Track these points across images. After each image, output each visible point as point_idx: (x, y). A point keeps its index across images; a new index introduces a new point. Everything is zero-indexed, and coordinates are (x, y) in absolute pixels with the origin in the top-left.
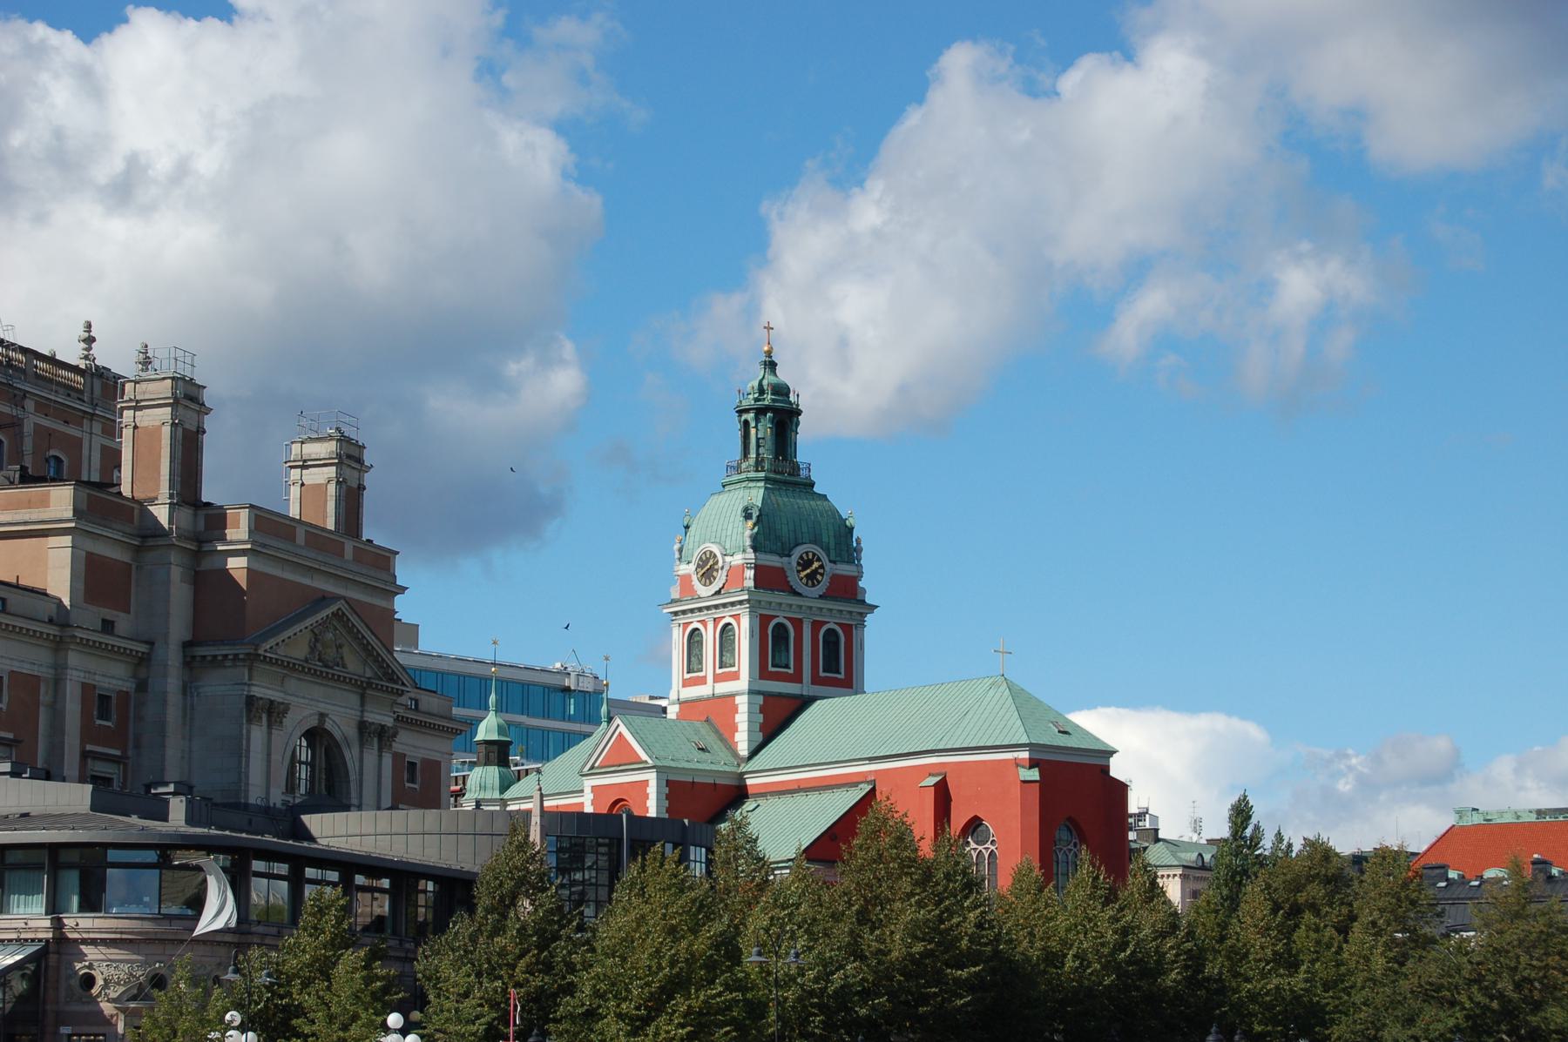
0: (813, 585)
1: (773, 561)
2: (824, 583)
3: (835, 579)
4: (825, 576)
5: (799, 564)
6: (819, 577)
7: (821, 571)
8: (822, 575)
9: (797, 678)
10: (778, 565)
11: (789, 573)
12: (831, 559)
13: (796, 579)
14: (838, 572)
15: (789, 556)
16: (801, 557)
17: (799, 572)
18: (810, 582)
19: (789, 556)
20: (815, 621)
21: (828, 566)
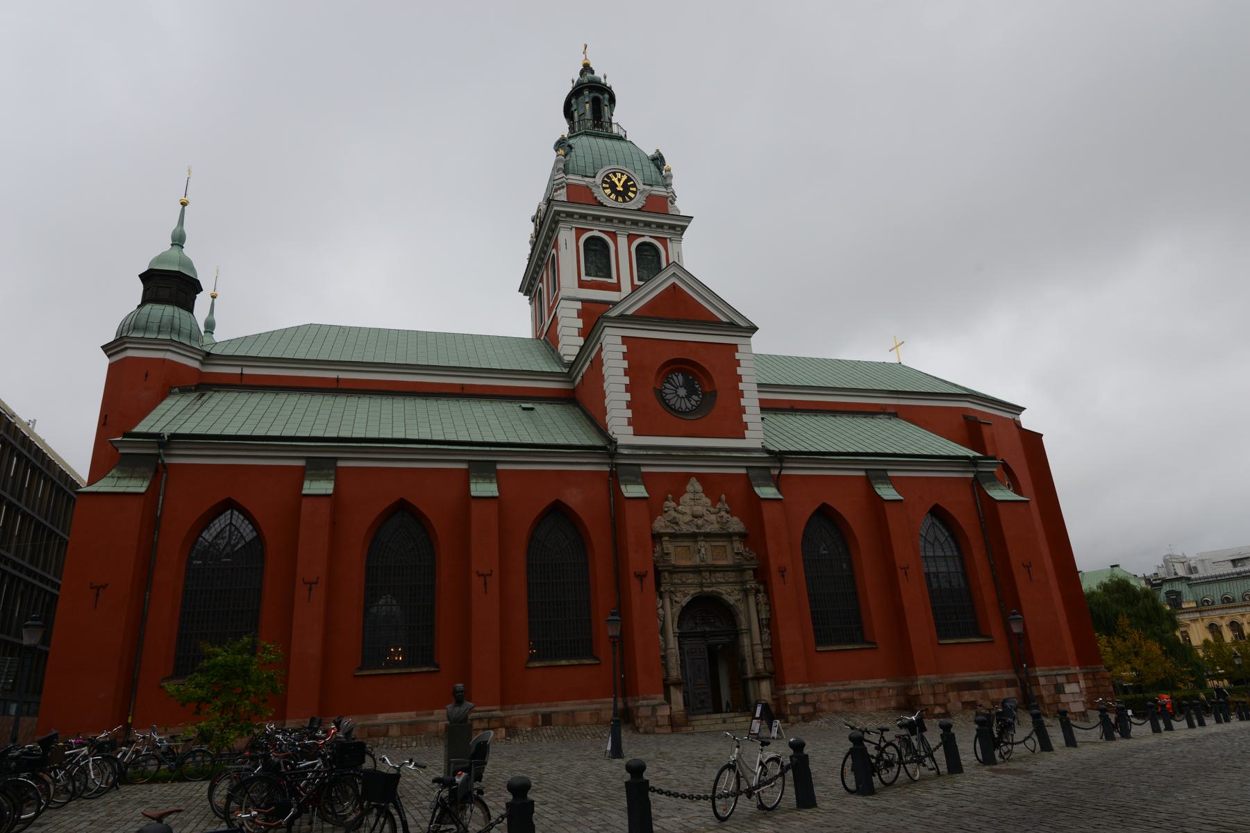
0: (624, 201)
1: (574, 179)
2: (637, 201)
3: (650, 198)
4: (638, 194)
5: (604, 182)
6: (630, 194)
7: (634, 189)
8: (635, 193)
9: (617, 288)
10: (585, 183)
11: (594, 190)
12: (646, 183)
13: (604, 195)
14: (653, 192)
15: (594, 177)
16: (607, 176)
17: (604, 188)
18: (620, 199)
19: (594, 177)
20: (630, 234)
21: (641, 186)
